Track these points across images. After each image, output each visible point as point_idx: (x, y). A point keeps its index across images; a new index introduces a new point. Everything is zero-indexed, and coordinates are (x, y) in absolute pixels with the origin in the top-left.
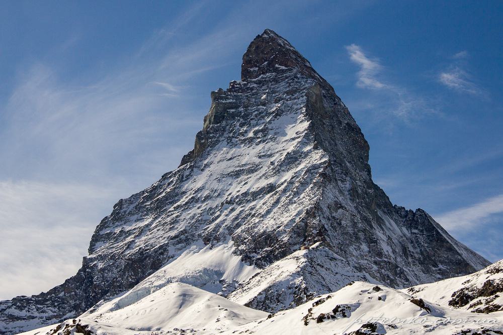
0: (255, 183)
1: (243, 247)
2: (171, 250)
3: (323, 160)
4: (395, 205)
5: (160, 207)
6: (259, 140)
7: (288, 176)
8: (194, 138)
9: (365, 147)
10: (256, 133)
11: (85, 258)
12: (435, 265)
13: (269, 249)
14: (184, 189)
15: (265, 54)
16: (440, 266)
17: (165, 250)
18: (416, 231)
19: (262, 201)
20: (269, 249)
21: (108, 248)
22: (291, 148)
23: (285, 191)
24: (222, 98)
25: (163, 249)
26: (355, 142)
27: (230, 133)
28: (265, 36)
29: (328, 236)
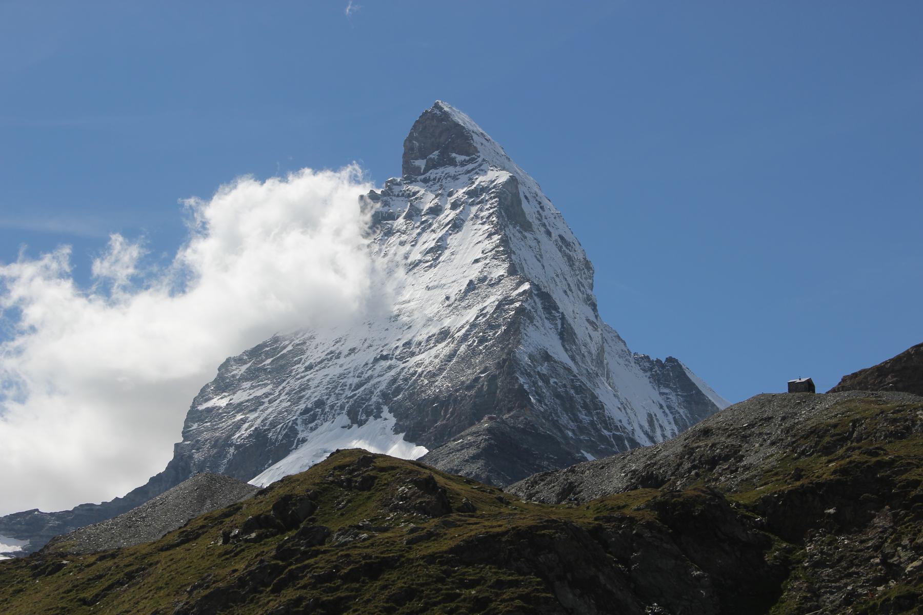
3: (521, 290)
11: (177, 445)
18: (667, 391)
22: (474, 273)
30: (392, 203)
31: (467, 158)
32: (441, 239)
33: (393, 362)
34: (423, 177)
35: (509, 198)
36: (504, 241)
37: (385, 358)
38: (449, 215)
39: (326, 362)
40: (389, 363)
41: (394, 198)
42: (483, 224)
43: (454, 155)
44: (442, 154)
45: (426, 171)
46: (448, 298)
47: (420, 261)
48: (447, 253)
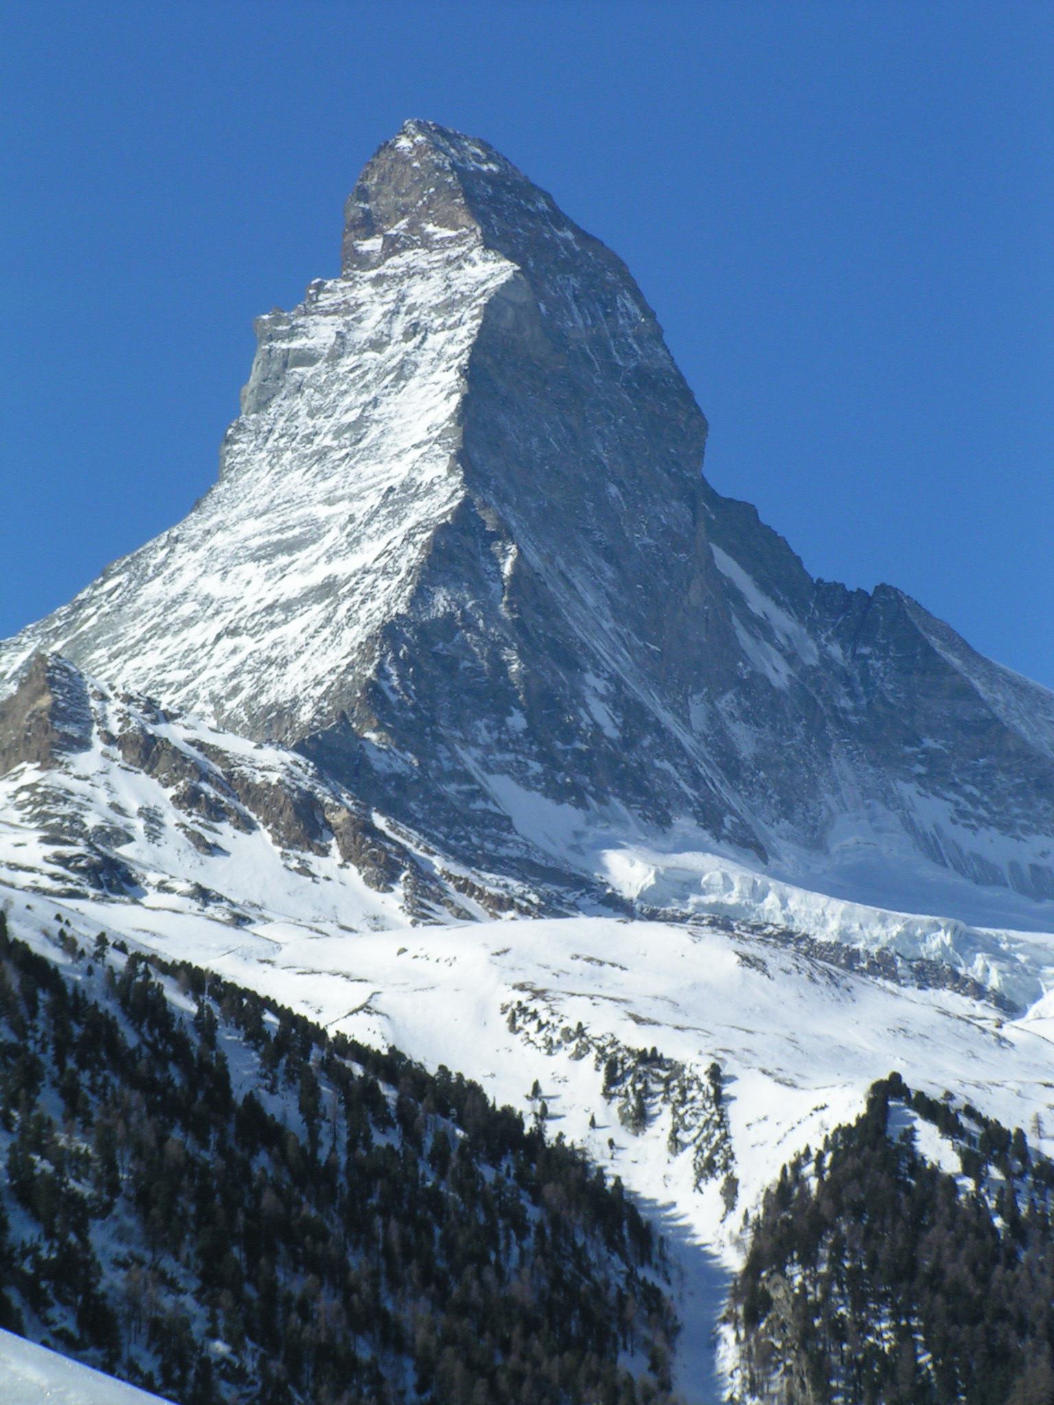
3: (446, 508)
4: (820, 581)
6: (345, 451)
10: (338, 434)
12: (914, 740)
15: (403, 195)
16: (929, 742)
18: (866, 650)
23: (352, 591)
27: (282, 436)
31: (452, 233)
32: (375, 403)
33: (246, 642)
34: (373, 273)
35: (510, 313)
37: (233, 632)
39: (141, 644)
40: (236, 641)
41: (317, 318)
43: (430, 228)
44: (412, 226)
46: (352, 519)
47: (331, 448)
48: (374, 431)
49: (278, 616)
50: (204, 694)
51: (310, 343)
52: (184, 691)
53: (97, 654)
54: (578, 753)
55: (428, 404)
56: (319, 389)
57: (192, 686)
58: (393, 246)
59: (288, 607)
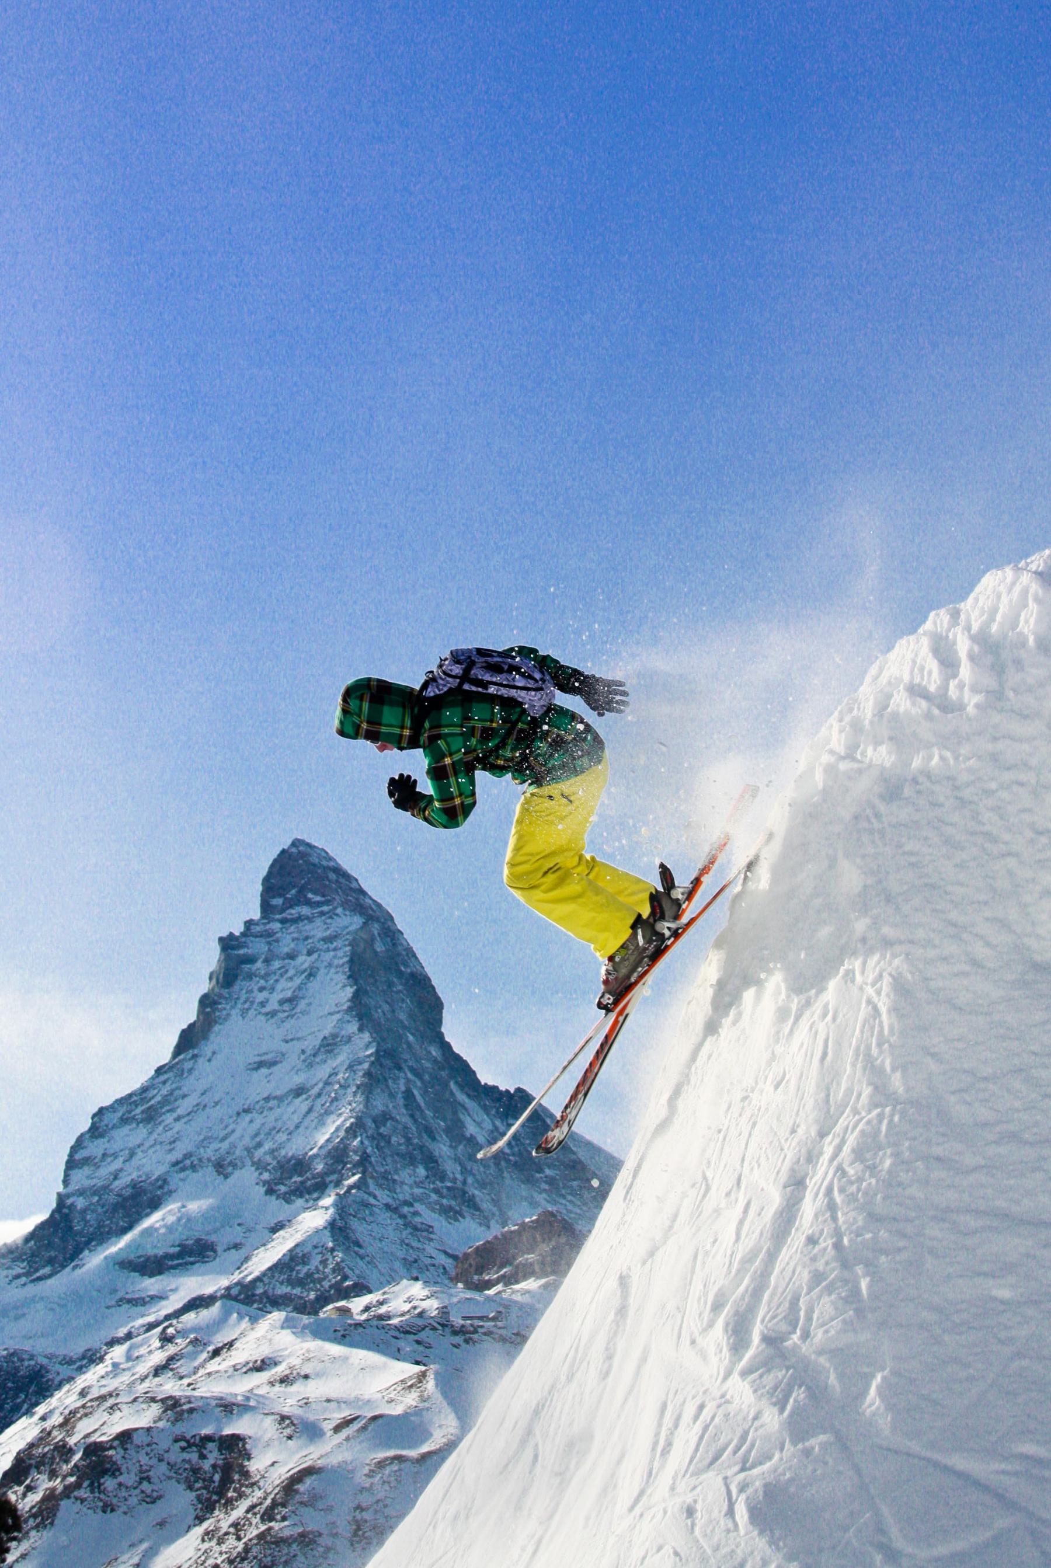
0: (284, 1078)
1: (266, 1176)
2: (175, 1180)
3: (368, 1052)
5: (151, 1116)
6: (286, 1014)
7: (322, 1072)
8: (196, 1004)
9: (437, 1006)
10: (282, 1002)
11: (59, 1194)
12: (540, 1170)
13: (299, 1179)
14: (185, 1090)
16: (548, 1172)
17: (165, 1181)
19: (291, 1109)
20: (299, 1179)
21: (88, 1177)
22: (328, 1029)
23: (319, 1095)
24: (233, 948)
25: (164, 1181)
26: (420, 1004)
27: (245, 1002)
28: (294, 850)
29: (370, 1163)
30: (251, 945)
32: (299, 988)
33: (255, 1115)
35: (362, 945)
36: (356, 997)
37: (247, 1111)
38: (304, 961)
41: (252, 939)
42: (337, 973)
43: (310, 895)
45: (282, 911)
46: (303, 1052)
48: (302, 1005)
49: (272, 1103)
50: (240, 1145)
51: (250, 951)
52: (227, 1142)
53: (164, 1117)
54: (448, 1188)
55: (334, 992)
56: (262, 977)
57: (232, 1139)
58: (290, 904)
59: (280, 1099)
